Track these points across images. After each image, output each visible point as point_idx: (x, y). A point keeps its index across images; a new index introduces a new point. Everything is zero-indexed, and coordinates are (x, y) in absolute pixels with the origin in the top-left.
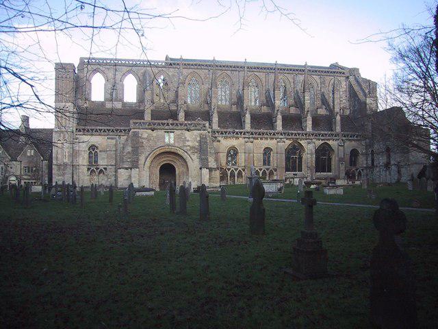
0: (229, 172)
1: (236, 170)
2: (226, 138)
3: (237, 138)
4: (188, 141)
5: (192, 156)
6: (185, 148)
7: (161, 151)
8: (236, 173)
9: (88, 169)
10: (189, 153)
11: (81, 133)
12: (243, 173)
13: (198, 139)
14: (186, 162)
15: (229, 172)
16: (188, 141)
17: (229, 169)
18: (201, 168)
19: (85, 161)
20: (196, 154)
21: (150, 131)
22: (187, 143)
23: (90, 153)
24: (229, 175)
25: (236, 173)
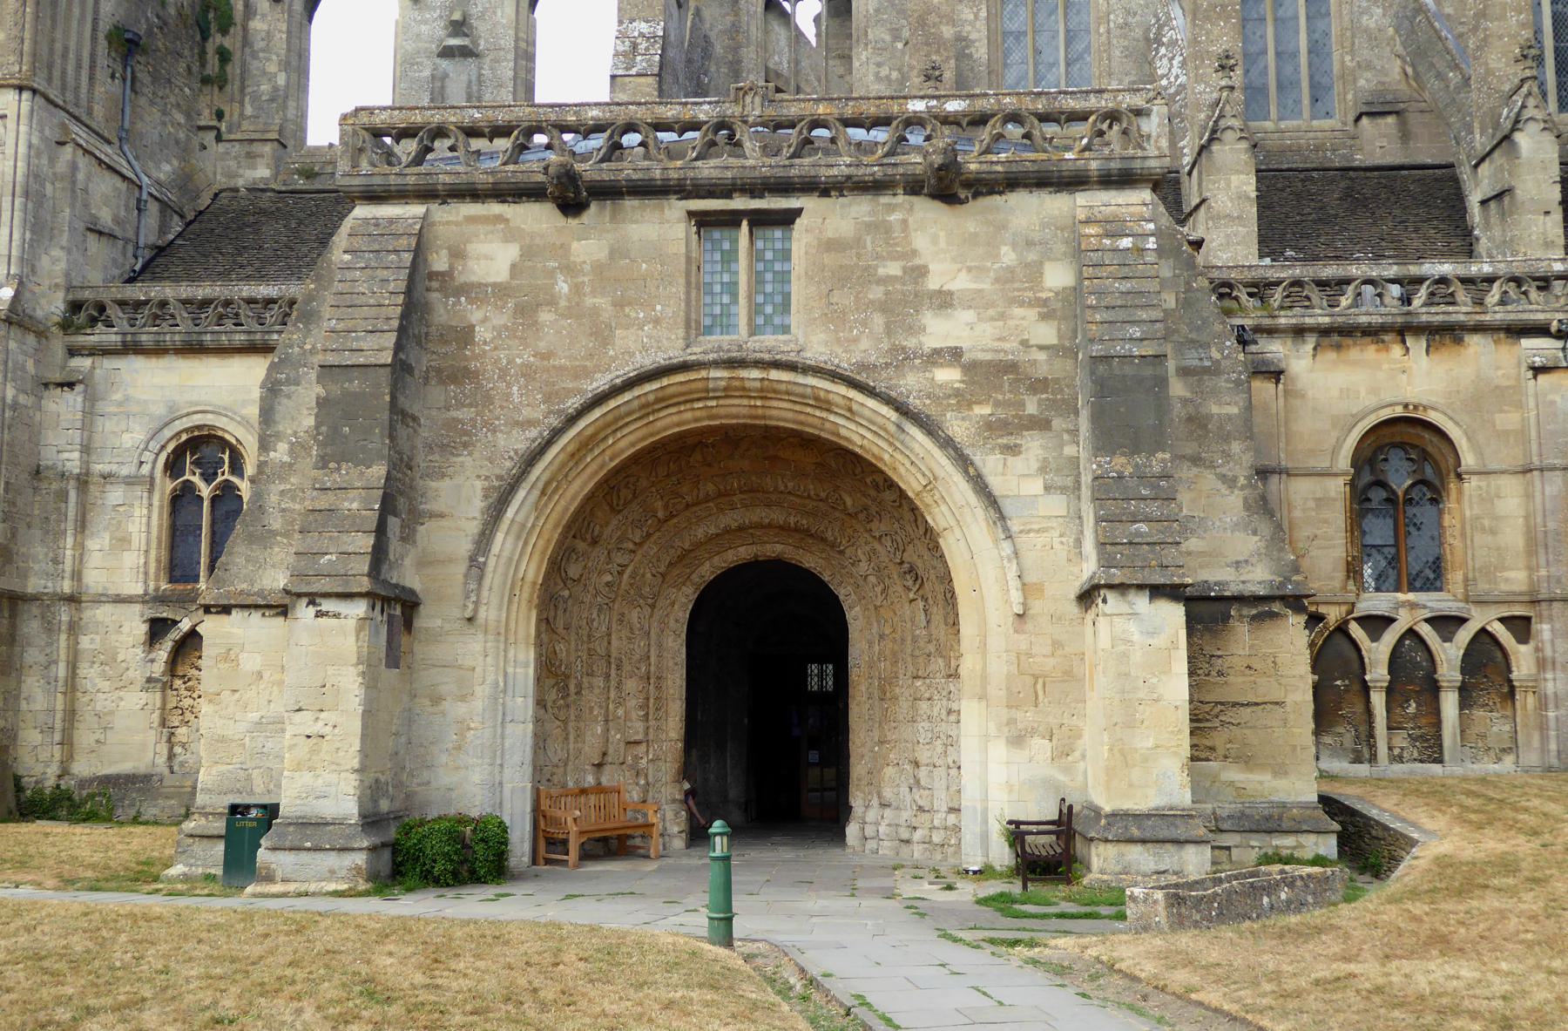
0: (1378, 653)
1: (1447, 624)
2: (1338, 335)
3: (1445, 334)
4: (944, 301)
5: (990, 464)
6: (910, 384)
7: (670, 422)
8: (1449, 655)
9: (158, 629)
10: (957, 427)
11: (111, 338)
12: (1522, 660)
13: (1058, 276)
14: (930, 538)
15: (1378, 653)
16: (944, 301)
17: (1377, 624)
18: (1087, 597)
19: (132, 559)
20: (1034, 446)
21: (538, 218)
22: (939, 331)
23: (182, 499)
24: (1378, 673)
25: (1449, 655)
